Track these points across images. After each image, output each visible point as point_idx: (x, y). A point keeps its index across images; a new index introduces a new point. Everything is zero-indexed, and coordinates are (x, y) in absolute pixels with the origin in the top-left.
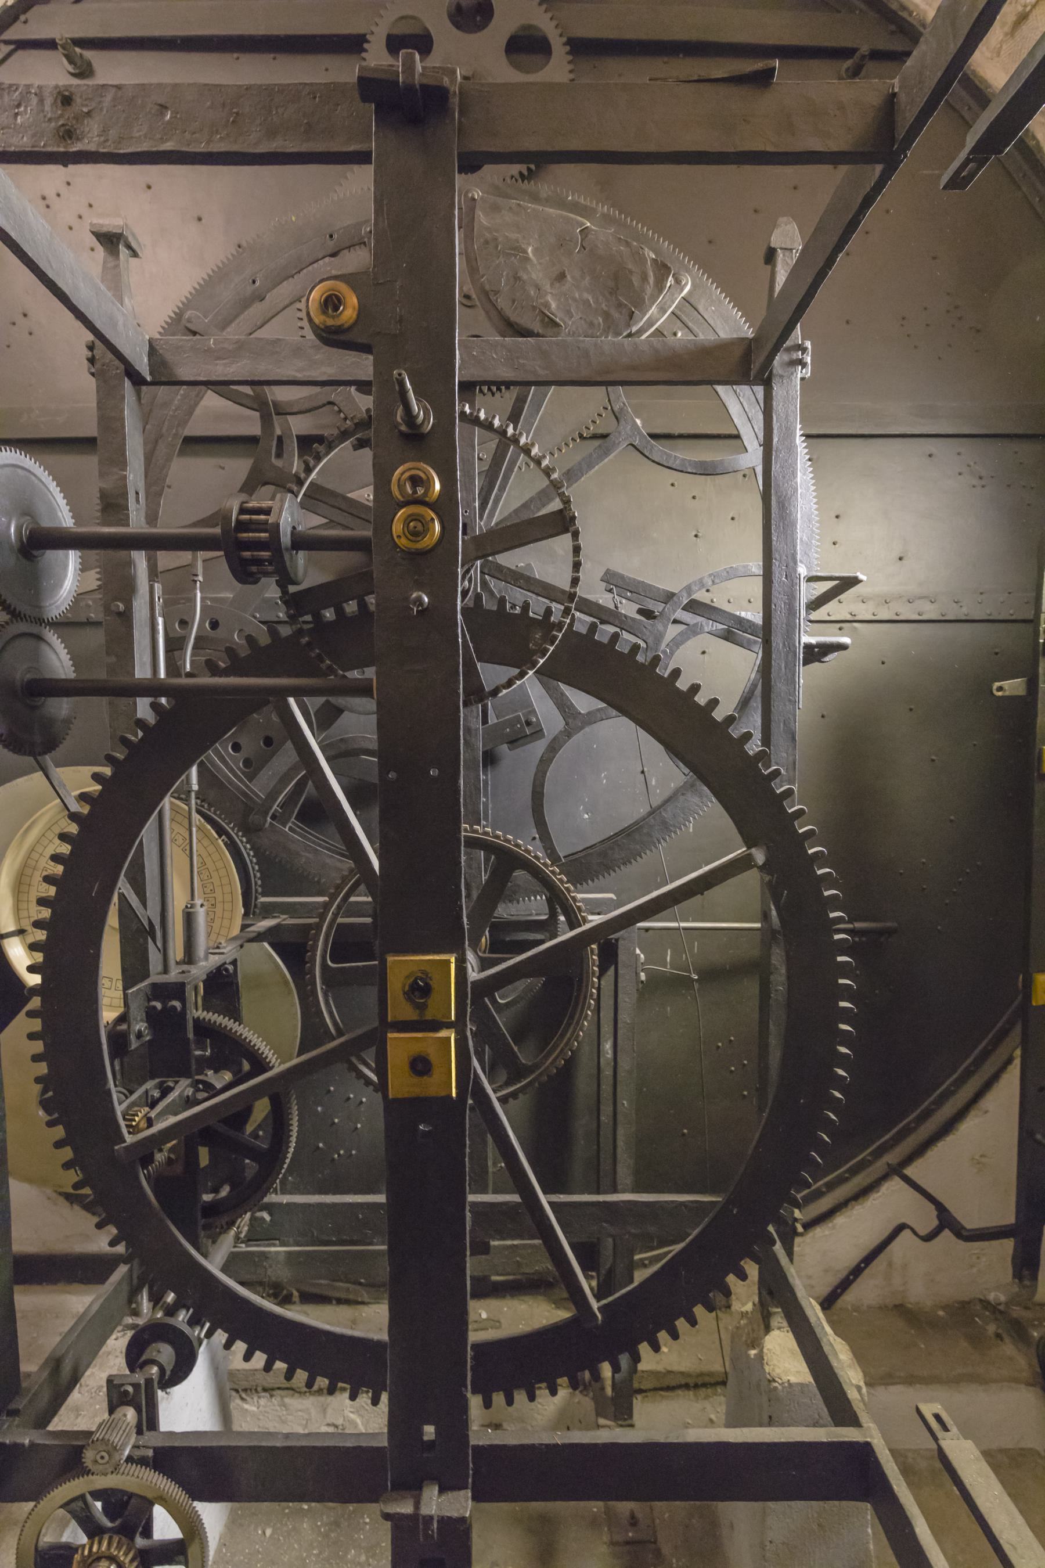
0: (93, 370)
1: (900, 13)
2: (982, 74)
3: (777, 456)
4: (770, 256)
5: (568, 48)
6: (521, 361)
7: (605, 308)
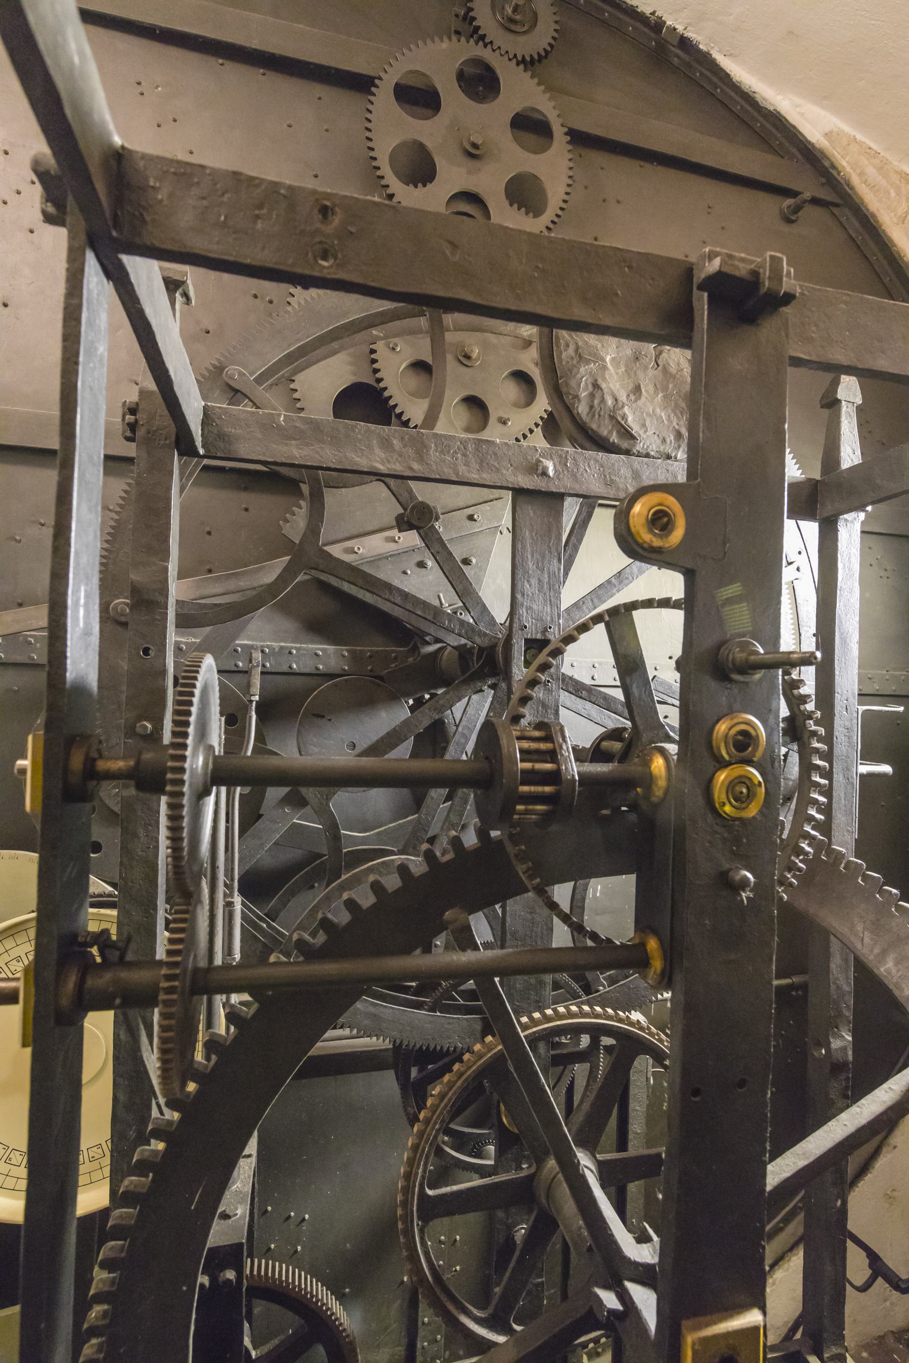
0: (128, 434)
1: (831, 170)
2: (889, 234)
3: (841, 595)
4: (832, 403)
5: (569, 138)
6: (613, 477)
7: (677, 427)
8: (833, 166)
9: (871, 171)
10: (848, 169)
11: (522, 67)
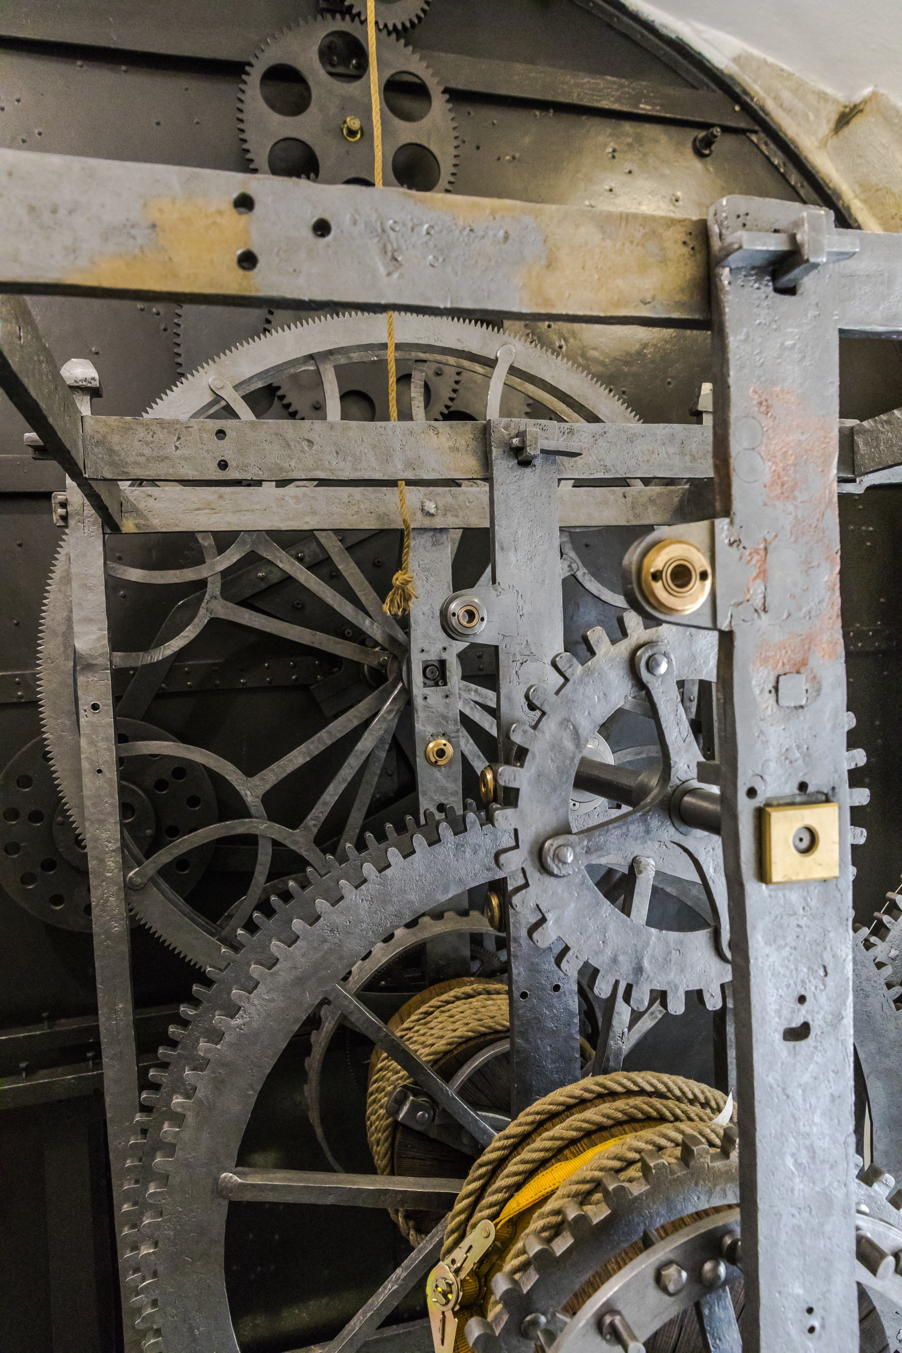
8: (746, 93)
9: (786, 95)
10: (762, 94)
11: (394, 36)
